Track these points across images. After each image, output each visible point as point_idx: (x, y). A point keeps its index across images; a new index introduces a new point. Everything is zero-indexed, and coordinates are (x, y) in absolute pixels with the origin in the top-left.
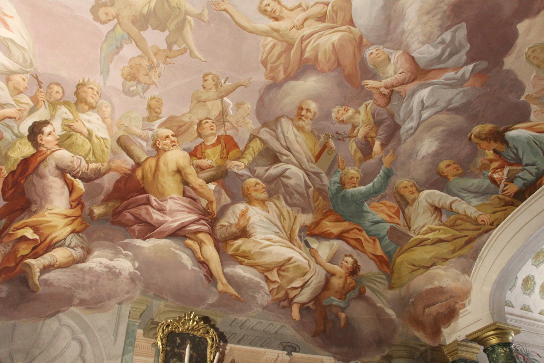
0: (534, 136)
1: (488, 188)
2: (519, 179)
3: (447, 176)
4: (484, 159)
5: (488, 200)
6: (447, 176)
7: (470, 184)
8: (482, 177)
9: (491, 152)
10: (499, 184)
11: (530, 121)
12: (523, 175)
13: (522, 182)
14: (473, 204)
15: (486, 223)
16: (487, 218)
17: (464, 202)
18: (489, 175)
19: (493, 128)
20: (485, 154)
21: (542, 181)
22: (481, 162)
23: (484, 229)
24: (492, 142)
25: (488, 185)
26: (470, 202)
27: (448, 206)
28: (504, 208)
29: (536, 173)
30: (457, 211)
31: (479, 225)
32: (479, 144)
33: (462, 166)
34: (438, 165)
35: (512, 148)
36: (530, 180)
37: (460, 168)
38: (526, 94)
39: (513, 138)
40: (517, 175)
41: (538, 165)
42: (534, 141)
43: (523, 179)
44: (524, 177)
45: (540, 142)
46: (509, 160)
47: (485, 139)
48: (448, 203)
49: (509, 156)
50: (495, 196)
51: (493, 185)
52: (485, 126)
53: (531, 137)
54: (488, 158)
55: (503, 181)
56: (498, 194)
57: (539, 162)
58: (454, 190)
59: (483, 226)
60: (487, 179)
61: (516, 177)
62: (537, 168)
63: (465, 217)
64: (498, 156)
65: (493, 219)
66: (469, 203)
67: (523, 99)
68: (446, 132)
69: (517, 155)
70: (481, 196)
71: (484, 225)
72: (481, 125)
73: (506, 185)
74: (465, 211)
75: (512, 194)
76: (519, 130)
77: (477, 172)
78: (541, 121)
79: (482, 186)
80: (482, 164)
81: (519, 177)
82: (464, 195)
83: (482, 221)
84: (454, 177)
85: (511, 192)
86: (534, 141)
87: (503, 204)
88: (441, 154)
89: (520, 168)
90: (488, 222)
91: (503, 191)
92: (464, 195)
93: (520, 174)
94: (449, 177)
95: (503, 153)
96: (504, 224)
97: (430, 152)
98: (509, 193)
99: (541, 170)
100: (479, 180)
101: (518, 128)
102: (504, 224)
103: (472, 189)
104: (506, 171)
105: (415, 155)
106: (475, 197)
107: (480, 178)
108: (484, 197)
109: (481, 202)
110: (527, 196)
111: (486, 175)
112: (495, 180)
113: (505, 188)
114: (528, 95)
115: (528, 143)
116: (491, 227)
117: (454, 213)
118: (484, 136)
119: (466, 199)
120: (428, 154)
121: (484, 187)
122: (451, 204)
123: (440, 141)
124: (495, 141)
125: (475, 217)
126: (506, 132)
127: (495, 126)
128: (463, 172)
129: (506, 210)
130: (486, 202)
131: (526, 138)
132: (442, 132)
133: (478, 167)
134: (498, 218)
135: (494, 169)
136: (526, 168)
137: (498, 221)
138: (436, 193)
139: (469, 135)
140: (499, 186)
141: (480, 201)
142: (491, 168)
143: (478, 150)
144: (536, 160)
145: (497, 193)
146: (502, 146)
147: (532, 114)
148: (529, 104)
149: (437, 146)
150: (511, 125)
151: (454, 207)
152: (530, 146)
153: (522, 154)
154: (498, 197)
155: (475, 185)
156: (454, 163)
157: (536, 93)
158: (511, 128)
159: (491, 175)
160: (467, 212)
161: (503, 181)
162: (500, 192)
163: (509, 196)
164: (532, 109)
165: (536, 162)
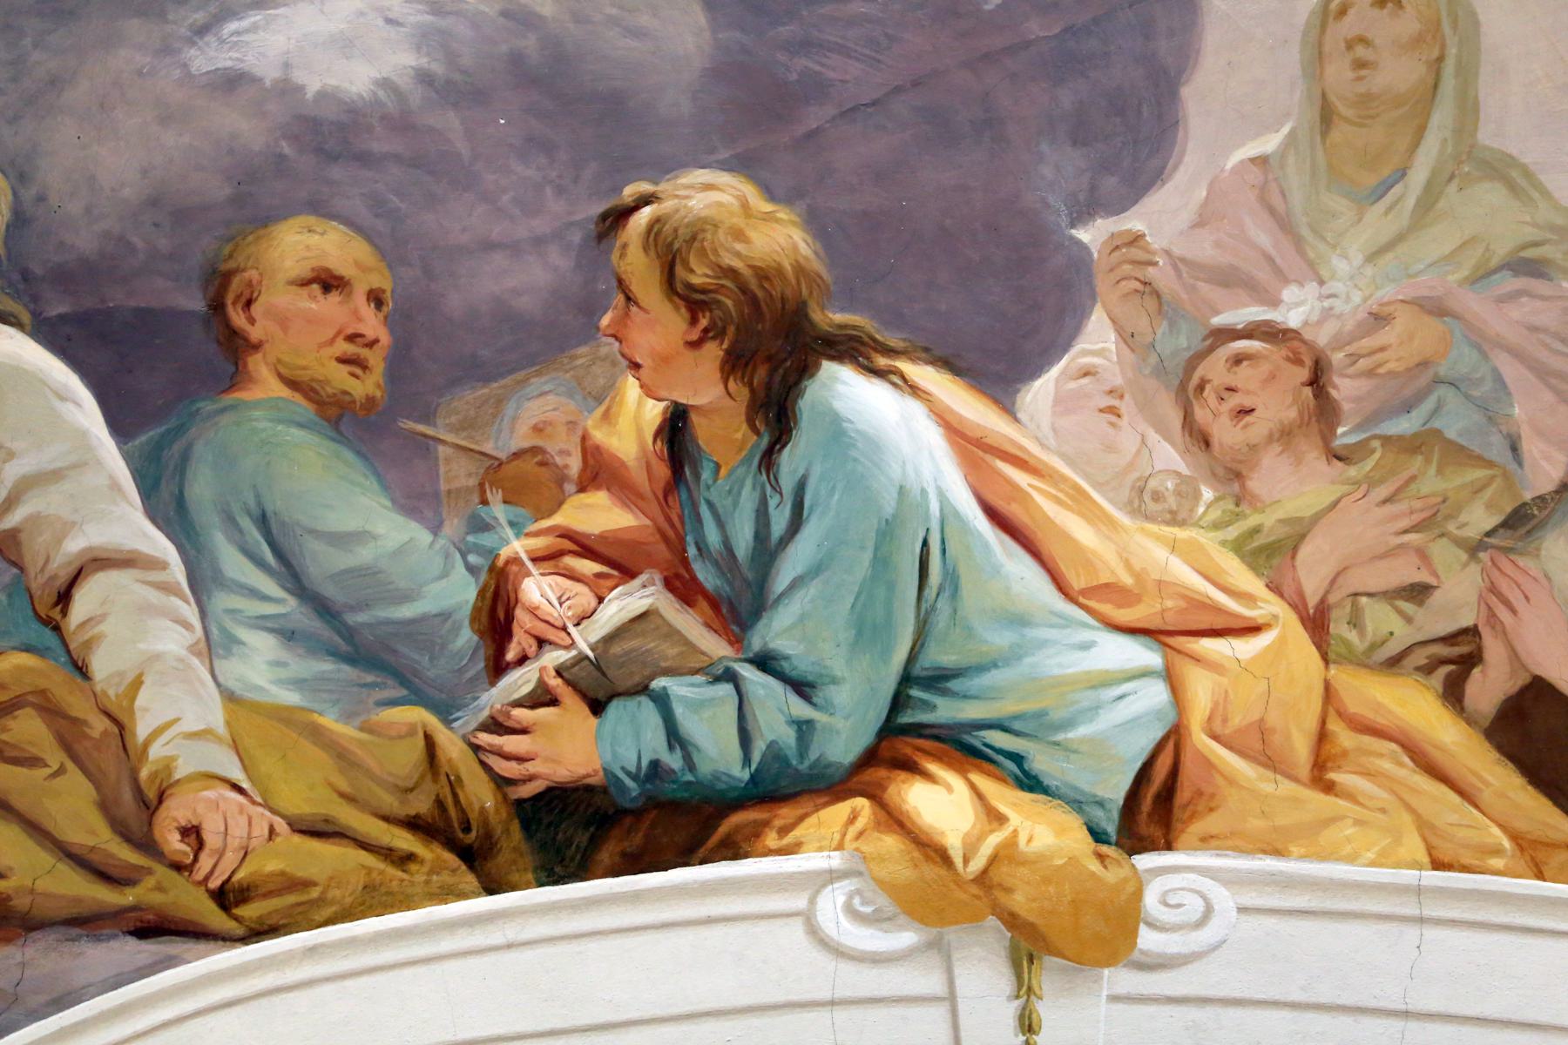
0: (949, 514)
1: (424, 632)
2: (647, 712)
3: (256, 347)
4: (572, 424)
5: (347, 717)
6: (256, 347)
7: (341, 520)
8: (453, 526)
9: (654, 412)
10: (511, 655)
11: (1008, 408)
12: (697, 706)
13: (653, 743)
14: (235, 671)
15: (205, 863)
16: (238, 830)
17: (190, 613)
18: (505, 553)
19: (799, 269)
20: (602, 397)
21: (766, 824)
22: (538, 429)
23: (157, 899)
24: (714, 352)
25: (444, 616)
26: (232, 641)
27: (54, 565)
28: (404, 841)
29: (775, 753)
30: (88, 645)
31: (147, 845)
32: (628, 299)
33: (400, 362)
34: (265, 220)
35: (777, 489)
36: (705, 768)
37: (376, 359)
38: (1131, 221)
39: (838, 431)
40: (658, 683)
41: (827, 708)
42: (925, 543)
43: (674, 736)
44: (690, 724)
45: (952, 580)
46: (701, 548)
47: (694, 302)
48: (74, 545)
49: (721, 524)
50: (417, 715)
51: (466, 638)
52: (768, 218)
53: (934, 507)
54: (599, 436)
55: (554, 657)
56: (448, 723)
57: (841, 696)
58: (202, 487)
59: (161, 872)
60: (471, 569)
61: (643, 689)
62: (804, 729)
63: (99, 725)
64: (663, 471)
65: (272, 866)
66: (213, 646)
67: (1091, 235)
68: (529, 44)
69: (767, 551)
70: (335, 654)
71: (178, 867)
72: (749, 191)
73: (542, 698)
74: (137, 683)
75: (531, 778)
76: (915, 408)
77: (458, 473)
78: (1064, 457)
79: (405, 597)
80: (535, 450)
81: (662, 702)
82: (234, 564)
83: (192, 833)
84: (285, 392)
85: (531, 768)
86: (925, 543)
87: (421, 805)
88: (364, 159)
89: (715, 647)
90: (217, 866)
91: (496, 725)
92: (234, 564)
93: (677, 688)
94: (258, 365)
95: (706, 475)
96: (312, 951)
97: (312, 86)
98: (520, 759)
99: (813, 755)
100: (425, 537)
101: (914, 390)
102: (312, 951)
103: (322, 563)
104: (624, 603)
105: (199, 17)
106: (288, 635)
107: (436, 530)
108: (347, 671)
109: (291, 698)
110: (605, 856)
111: (486, 540)
112: (510, 617)
113: (522, 715)
114: (1136, 239)
115: (888, 532)
116: (213, 917)
117: (49, 637)
118: (700, 275)
119: (222, 601)
120: (287, 89)
121: (406, 612)
122: (98, 562)
123: (438, 68)
124: (734, 364)
125: (167, 766)
126: (839, 357)
127: (817, 266)
128: (370, 401)
129: (404, 860)
130: (329, 721)
131: (902, 491)
132: (505, 14)
133: (488, 448)
134: (307, 884)
135: (567, 534)
136: (748, 672)
137: (291, 899)
138: (67, 409)
139: (630, 192)
140: (498, 668)
141: (298, 684)
142: (557, 520)
143: (589, 332)
144: (838, 666)
145: (445, 712)
146: (741, 431)
147: (1055, 371)
148: (1093, 297)
149: (385, 83)
150: (894, 341)
151: (83, 604)
152: (882, 563)
153: (799, 570)
154: (430, 744)
155: (364, 555)
156: (376, 298)
157: (1177, 262)
158: (882, 362)
159: (516, 560)
160: (142, 700)
161: (554, 657)
162: (468, 720)
163: (502, 782)
164: (1078, 347)
165: (834, 681)
